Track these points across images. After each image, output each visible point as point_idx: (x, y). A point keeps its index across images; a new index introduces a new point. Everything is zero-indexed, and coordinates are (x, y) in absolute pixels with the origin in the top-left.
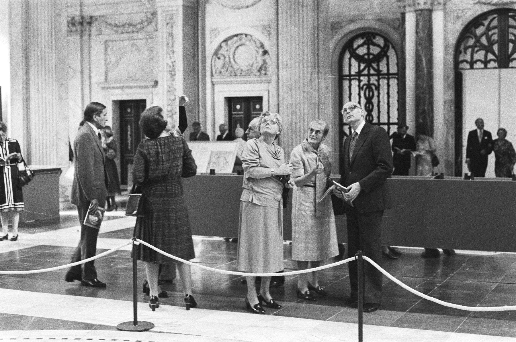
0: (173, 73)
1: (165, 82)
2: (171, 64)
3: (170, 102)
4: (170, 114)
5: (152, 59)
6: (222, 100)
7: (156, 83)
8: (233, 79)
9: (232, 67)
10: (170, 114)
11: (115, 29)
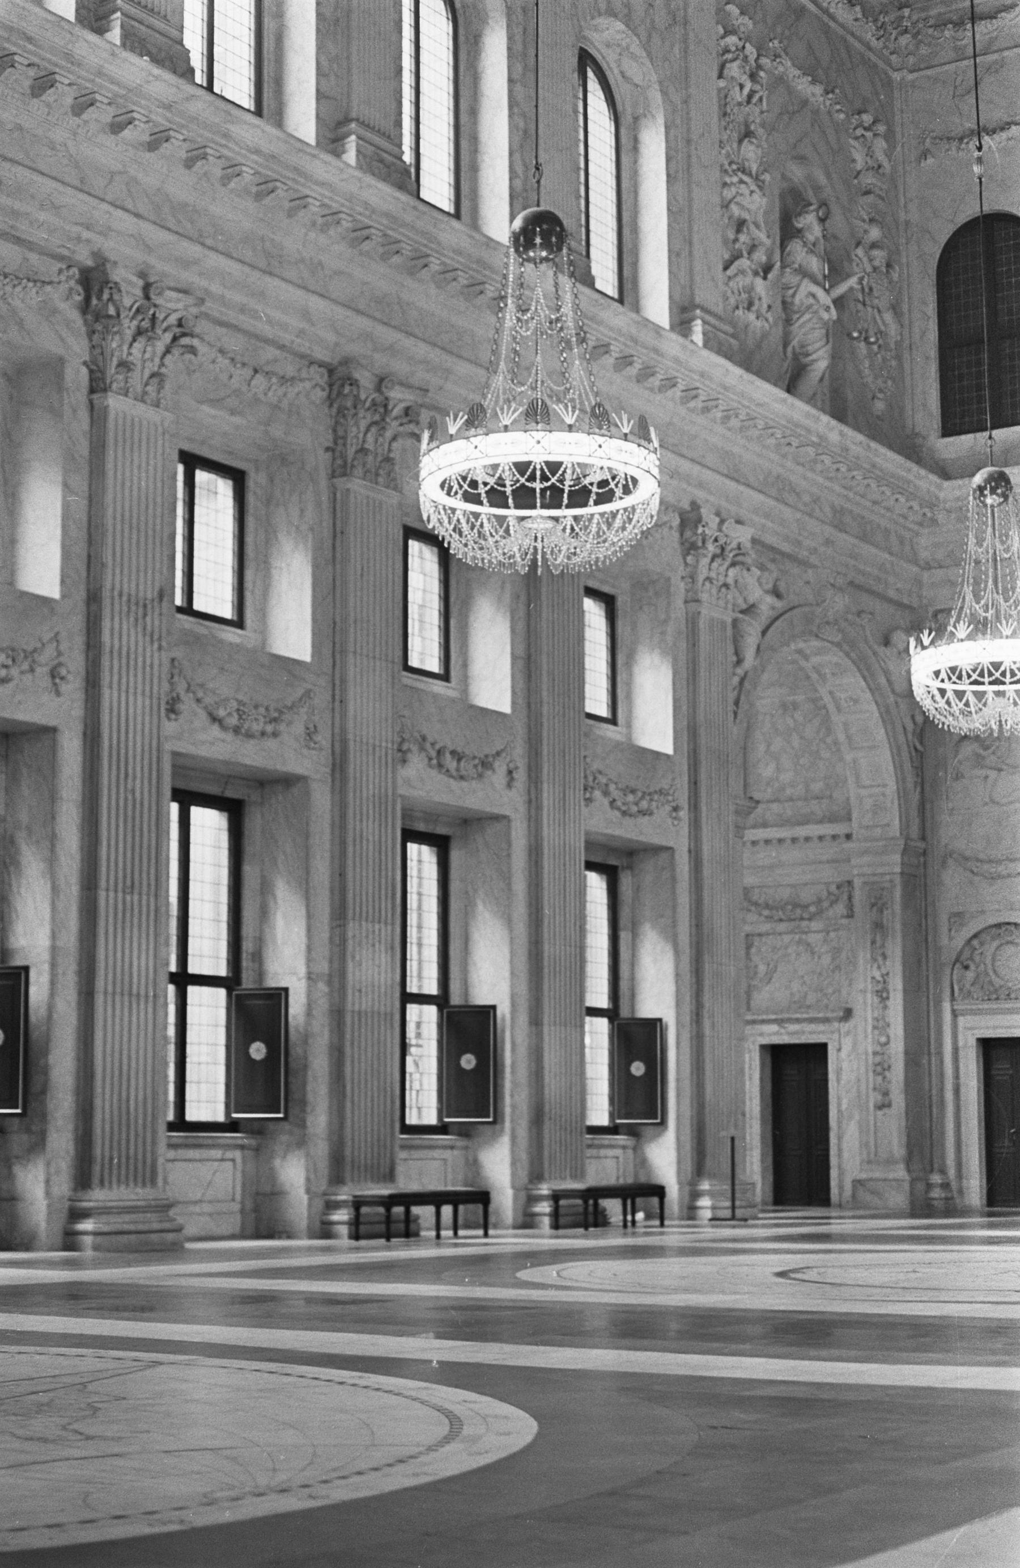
0: (885, 995)
1: (869, 1012)
2: (879, 978)
3: (878, 1049)
4: (879, 1069)
5: (838, 968)
6: (972, 1042)
7: (848, 1014)
8: (994, 1006)
9: (991, 983)
10: (879, 1069)
11: (766, 912)
